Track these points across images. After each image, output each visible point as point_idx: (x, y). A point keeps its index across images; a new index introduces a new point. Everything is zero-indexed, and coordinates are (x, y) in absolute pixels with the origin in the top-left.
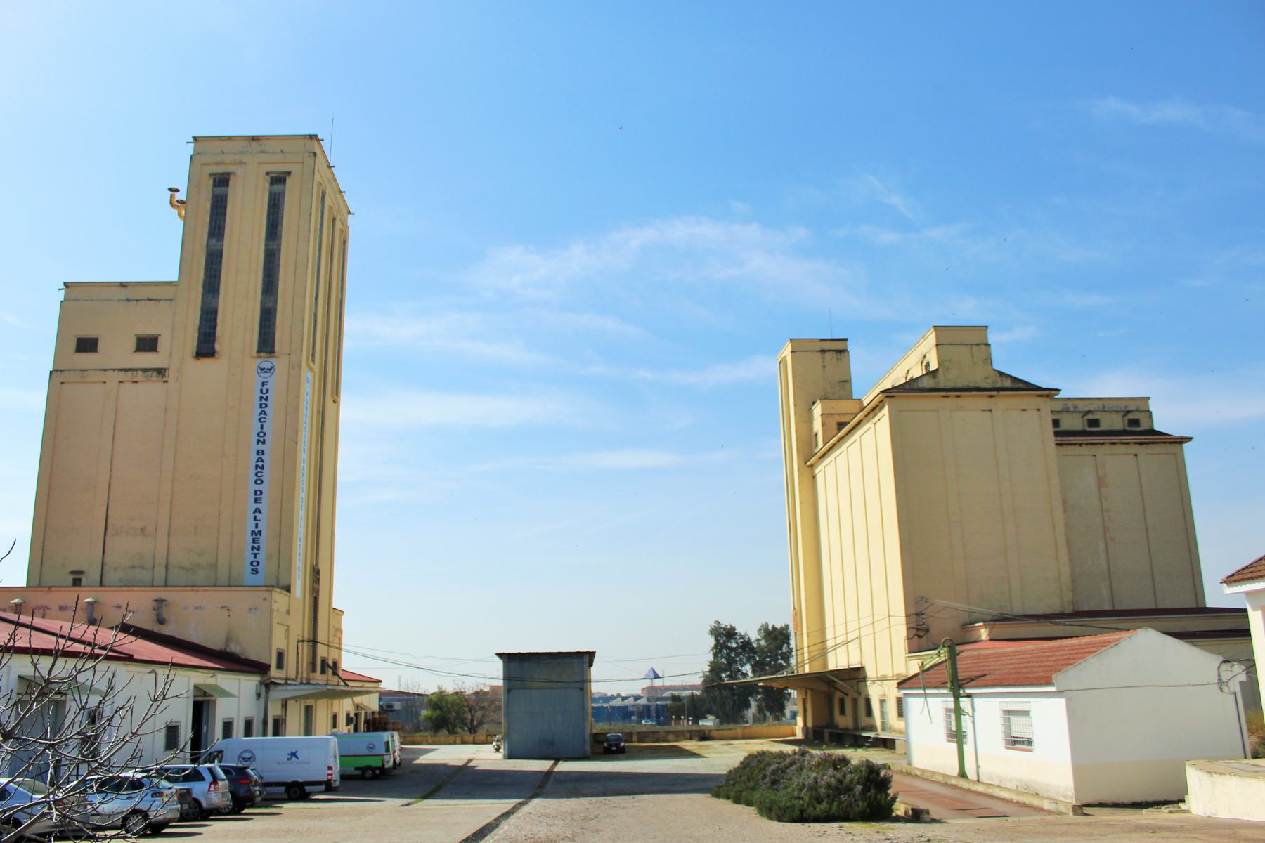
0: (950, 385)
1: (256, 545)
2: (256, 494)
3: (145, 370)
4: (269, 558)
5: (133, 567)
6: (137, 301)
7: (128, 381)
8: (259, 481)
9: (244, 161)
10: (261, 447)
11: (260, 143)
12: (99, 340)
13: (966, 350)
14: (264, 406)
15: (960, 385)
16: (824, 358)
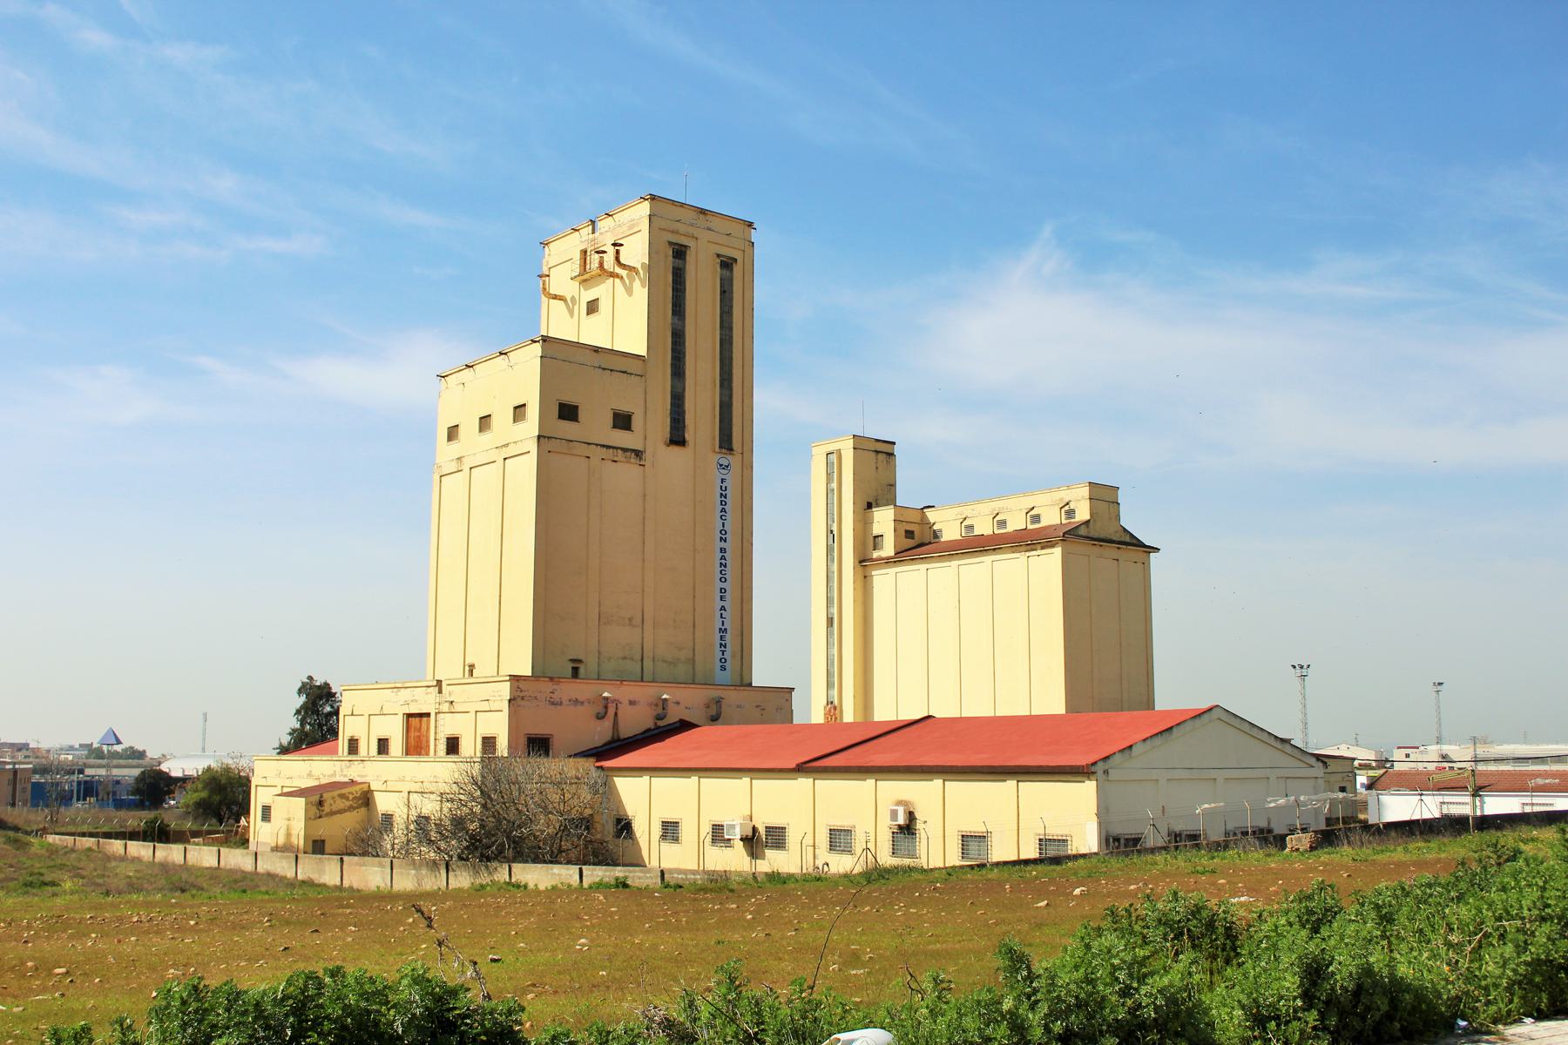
0: (1096, 535)
1: (723, 643)
2: (721, 592)
3: (625, 450)
4: (733, 656)
5: (624, 658)
6: (611, 370)
7: (608, 460)
8: (723, 580)
9: (695, 235)
10: (723, 545)
11: (708, 217)
12: (580, 408)
13: (1107, 504)
14: (723, 503)
15: (1101, 536)
16: (877, 459)
